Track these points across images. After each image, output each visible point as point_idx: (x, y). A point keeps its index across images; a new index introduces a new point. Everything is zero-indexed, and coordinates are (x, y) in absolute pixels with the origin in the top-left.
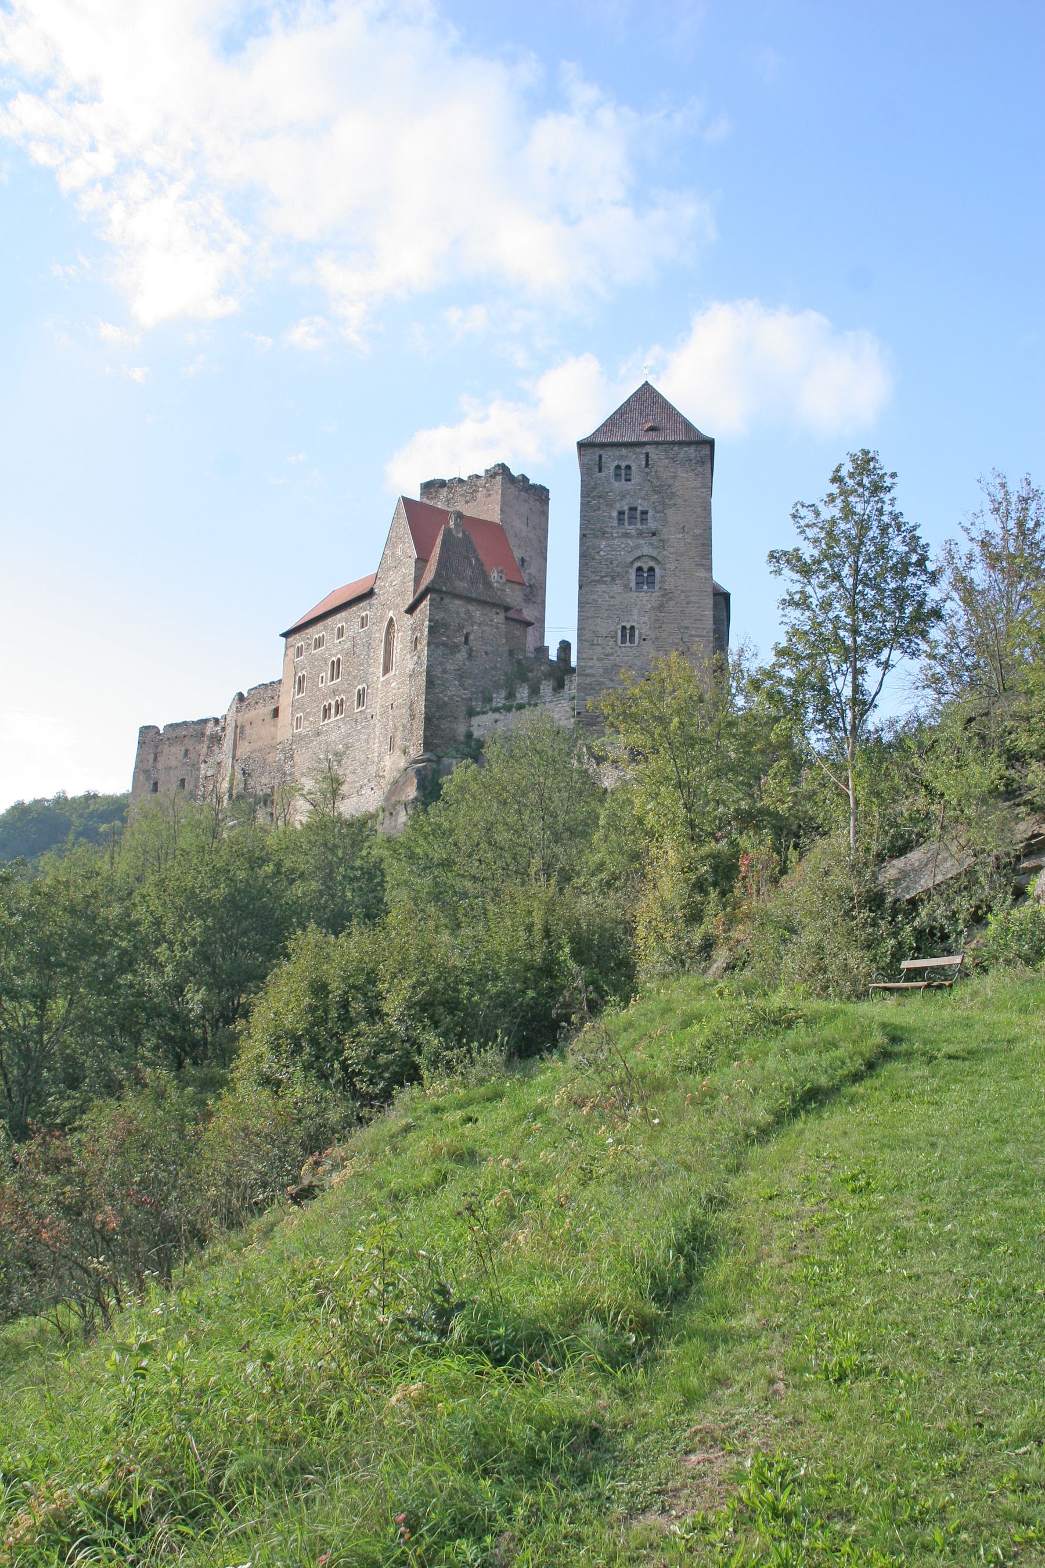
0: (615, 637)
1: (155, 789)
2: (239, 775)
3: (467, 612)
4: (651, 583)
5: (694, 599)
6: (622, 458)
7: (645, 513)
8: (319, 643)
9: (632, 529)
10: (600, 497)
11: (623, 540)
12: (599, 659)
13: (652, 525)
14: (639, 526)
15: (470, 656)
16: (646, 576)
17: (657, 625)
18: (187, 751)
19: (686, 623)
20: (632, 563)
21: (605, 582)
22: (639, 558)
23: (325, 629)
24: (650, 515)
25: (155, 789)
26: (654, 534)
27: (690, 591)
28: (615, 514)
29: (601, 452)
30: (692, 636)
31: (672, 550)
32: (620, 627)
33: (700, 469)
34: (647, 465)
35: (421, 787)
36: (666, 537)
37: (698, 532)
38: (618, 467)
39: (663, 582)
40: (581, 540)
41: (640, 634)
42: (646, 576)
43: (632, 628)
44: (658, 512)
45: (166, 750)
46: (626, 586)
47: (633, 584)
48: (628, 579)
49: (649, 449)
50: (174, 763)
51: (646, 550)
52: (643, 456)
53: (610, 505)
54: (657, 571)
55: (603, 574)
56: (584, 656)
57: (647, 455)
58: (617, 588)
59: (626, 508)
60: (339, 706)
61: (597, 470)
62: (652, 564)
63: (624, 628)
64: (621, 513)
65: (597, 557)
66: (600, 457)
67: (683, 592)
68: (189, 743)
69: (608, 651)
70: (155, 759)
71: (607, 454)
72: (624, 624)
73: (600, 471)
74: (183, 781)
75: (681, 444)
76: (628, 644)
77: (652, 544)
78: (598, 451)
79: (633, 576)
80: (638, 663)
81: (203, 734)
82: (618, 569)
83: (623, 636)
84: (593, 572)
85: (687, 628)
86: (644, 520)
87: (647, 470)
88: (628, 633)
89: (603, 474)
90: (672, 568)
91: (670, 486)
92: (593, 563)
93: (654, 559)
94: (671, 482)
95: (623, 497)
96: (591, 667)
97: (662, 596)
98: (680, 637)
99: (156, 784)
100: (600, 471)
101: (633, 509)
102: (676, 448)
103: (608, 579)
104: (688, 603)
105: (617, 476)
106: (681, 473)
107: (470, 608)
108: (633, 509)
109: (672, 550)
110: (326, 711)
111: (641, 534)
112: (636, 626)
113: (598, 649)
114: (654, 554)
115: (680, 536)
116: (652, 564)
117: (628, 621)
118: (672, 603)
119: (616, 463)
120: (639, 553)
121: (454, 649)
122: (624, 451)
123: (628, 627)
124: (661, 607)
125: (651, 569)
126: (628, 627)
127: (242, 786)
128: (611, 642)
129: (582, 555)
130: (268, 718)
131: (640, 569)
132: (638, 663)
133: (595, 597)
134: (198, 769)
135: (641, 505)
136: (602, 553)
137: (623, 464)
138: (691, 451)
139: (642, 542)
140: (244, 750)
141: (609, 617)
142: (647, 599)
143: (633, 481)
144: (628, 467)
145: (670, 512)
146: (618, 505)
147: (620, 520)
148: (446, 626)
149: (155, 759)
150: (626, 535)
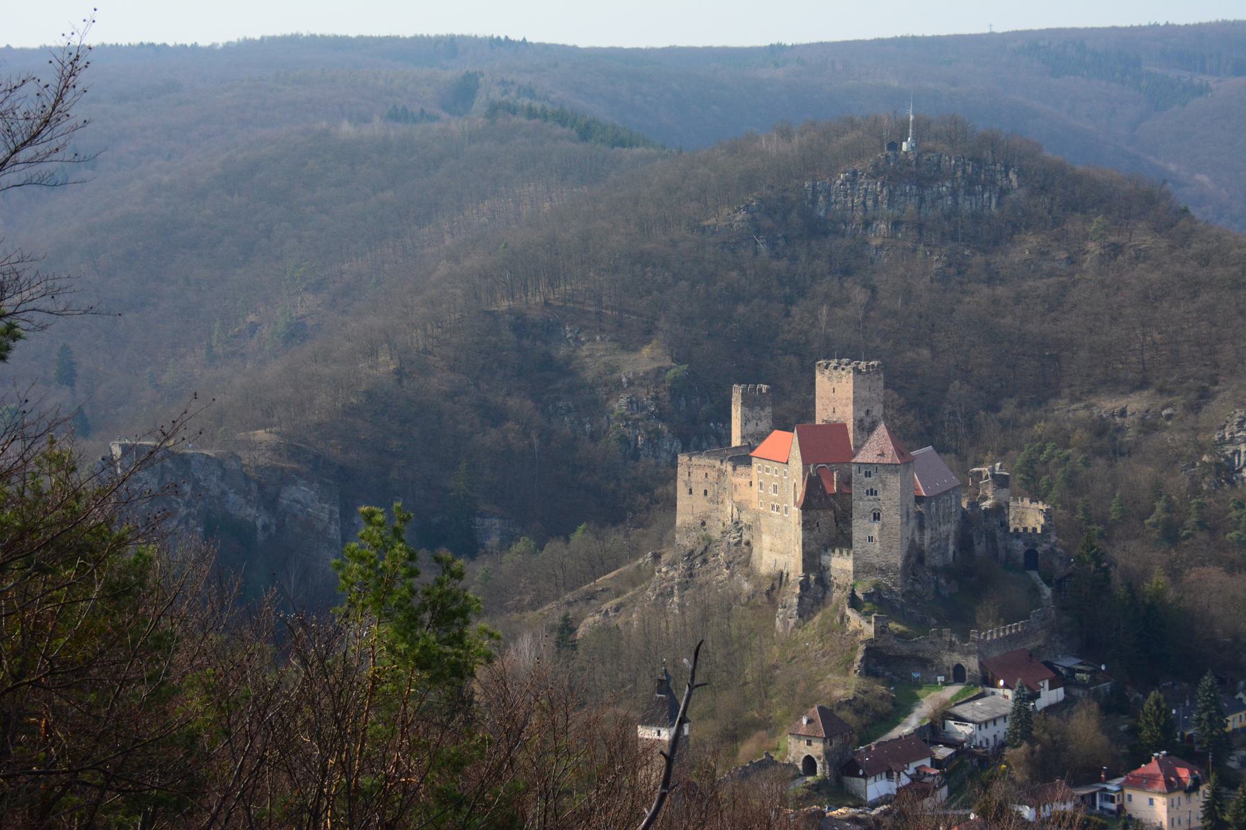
1: (691, 492)
2: (735, 510)
3: (818, 514)
4: (879, 520)
6: (868, 468)
7: (876, 491)
8: (767, 470)
9: (871, 497)
13: (879, 496)
15: (819, 531)
18: (706, 474)
23: (770, 465)
25: (691, 492)
35: (801, 589)
42: (877, 517)
45: (695, 471)
46: (870, 520)
50: (700, 481)
54: (881, 515)
58: (866, 521)
60: (778, 508)
64: (867, 491)
68: (708, 470)
70: (689, 475)
74: (706, 491)
79: (872, 517)
81: (714, 467)
86: (876, 494)
88: (871, 539)
99: (691, 490)
101: (872, 490)
106: (889, 476)
107: (818, 511)
108: (872, 490)
110: (773, 507)
111: (875, 500)
121: (812, 530)
124: (882, 529)
125: (879, 514)
127: (737, 516)
130: (748, 485)
131: (875, 514)
134: (713, 486)
140: (737, 498)
142: (876, 526)
148: (809, 522)
149: (689, 475)
150: (869, 500)
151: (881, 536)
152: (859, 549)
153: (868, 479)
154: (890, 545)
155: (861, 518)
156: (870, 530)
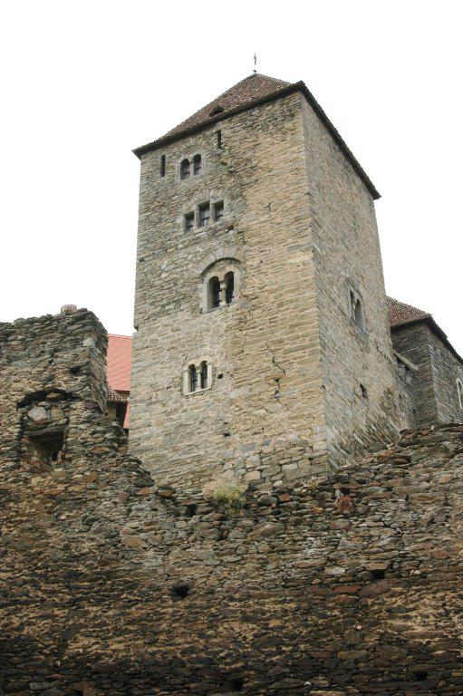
0: (181, 384)
5: (288, 297)
6: (188, 150)
7: (219, 206)
10: (163, 205)
11: (187, 250)
12: (160, 424)
13: (227, 216)
14: (211, 223)
16: (221, 290)
17: (236, 350)
19: (278, 335)
20: (204, 274)
21: (167, 313)
22: (212, 265)
24: (225, 205)
26: (231, 228)
27: (282, 288)
28: (180, 220)
29: (164, 153)
30: (286, 352)
31: (256, 240)
32: (186, 368)
33: (288, 125)
34: (220, 144)
36: (244, 226)
37: (289, 205)
38: (185, 164)
39: (243, 286)
40: (138, 266)
41: (215, 369)
42: (221, 290)
43: (204, 365)
44: (237, 197)
47: (204, 304)
48: (198, 298)
49: (220, 126)
51: (221, 253)
52: (216, 136)
53: (173, 212)
54: (237, 276)
55: (165, 302)
56: (139, 423)
57: (219, 133)
58: (183, 315)
59: (194, 208)
61: (159, 175)
62: (229, 268)
63: (192, 368)
64: (189, 217)
65: (157, 282)
66: (163, 158)
67: (271, 292)
69: (171, 406)
71: (167, 152)
72: (191, 363)
73: (163, 174)
75: (260, 103)
76: (198, 389)
77: (228, 242)
78: (158, 155)
80: (212, 414)
82: (183, 291)
83: (193, 381)
84: (151, 304)
85: (281, 342)
87: (220, 151)
88: (198, 374)
89: (166, 177)
90: (255, 262)
91: (249, 160)
92: (153, 292)
93: (232, 260)
94: (249, 154)
95: (190, 194)
96: (148, 438)
97: (242, 306)
98: (271, 355)
100: (163, 174)
101: (204, 207)
102: (256, 112)
103: (172, 306)
104: (281, 305)
105: (184, 174)
106: (265, 140)
109: (256, 240)
111: (214, 233)
112: (209, 359)
113: (159, 408)
114: (231, 253)
115: (266, 216)
116: (229, 268)
117: (198, 357)
118: (256, 313)
119: (182, 158)
120: (212, 259)
122: (191, 141)
123: (197, 364)
125: (230, 276)
126: (197, 364)
128: (176, 393)
129: (140, 285)
131: (215, 284)
132: (212, 414)
133: (154, 336)
135: (213, 196)
136: (164, 275)
137: (190, 157)
138: (276, 108)
139: (214, 243)
141: (172, 358)
142: (224, 316)
143: (202, 172)
144: (198, 159)
145: (249, 192)
146: (184, 209)
147: (188, 227)
150: (197, 241)
151: (237, 350)
152: (147, 433)
153: (184, 185)
154: (276, 372)
155: (163, 312)
156: (196, 342)
